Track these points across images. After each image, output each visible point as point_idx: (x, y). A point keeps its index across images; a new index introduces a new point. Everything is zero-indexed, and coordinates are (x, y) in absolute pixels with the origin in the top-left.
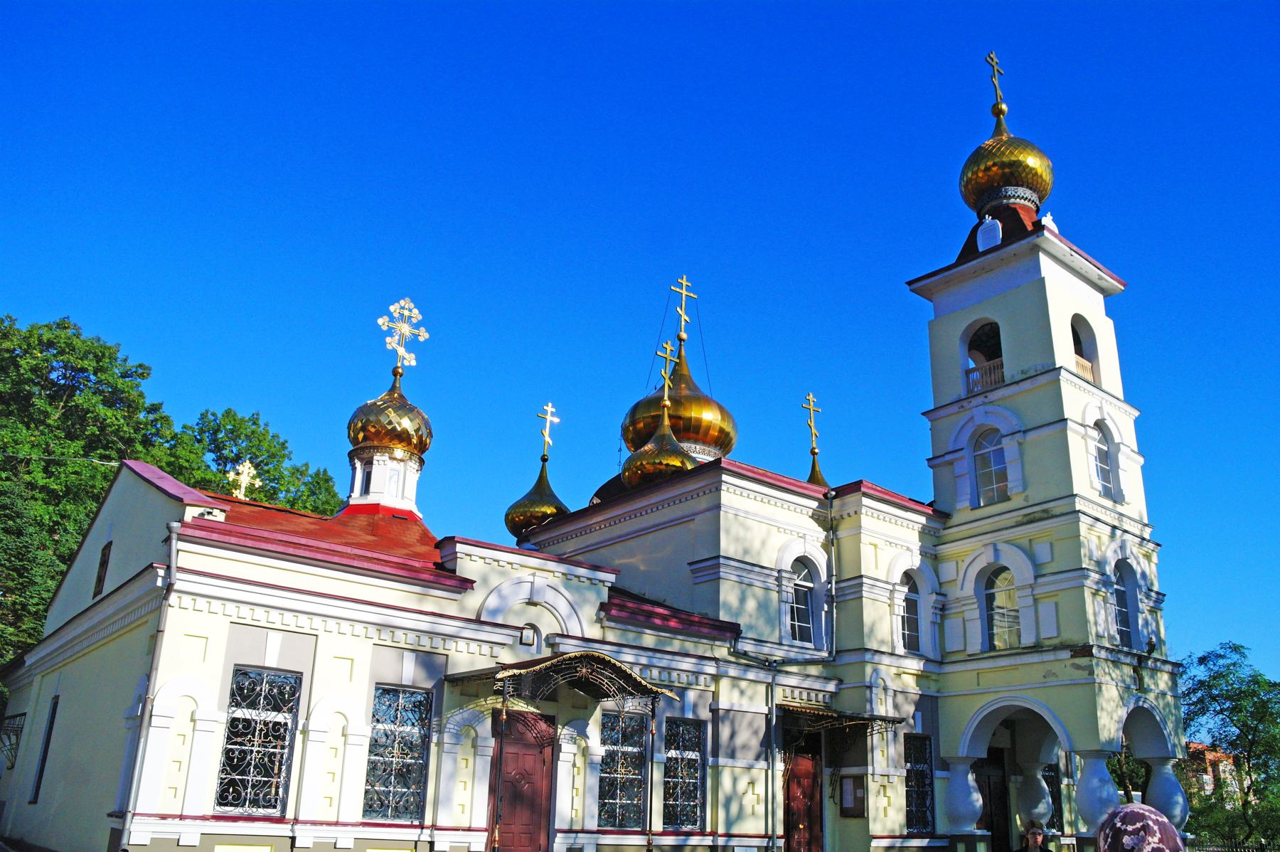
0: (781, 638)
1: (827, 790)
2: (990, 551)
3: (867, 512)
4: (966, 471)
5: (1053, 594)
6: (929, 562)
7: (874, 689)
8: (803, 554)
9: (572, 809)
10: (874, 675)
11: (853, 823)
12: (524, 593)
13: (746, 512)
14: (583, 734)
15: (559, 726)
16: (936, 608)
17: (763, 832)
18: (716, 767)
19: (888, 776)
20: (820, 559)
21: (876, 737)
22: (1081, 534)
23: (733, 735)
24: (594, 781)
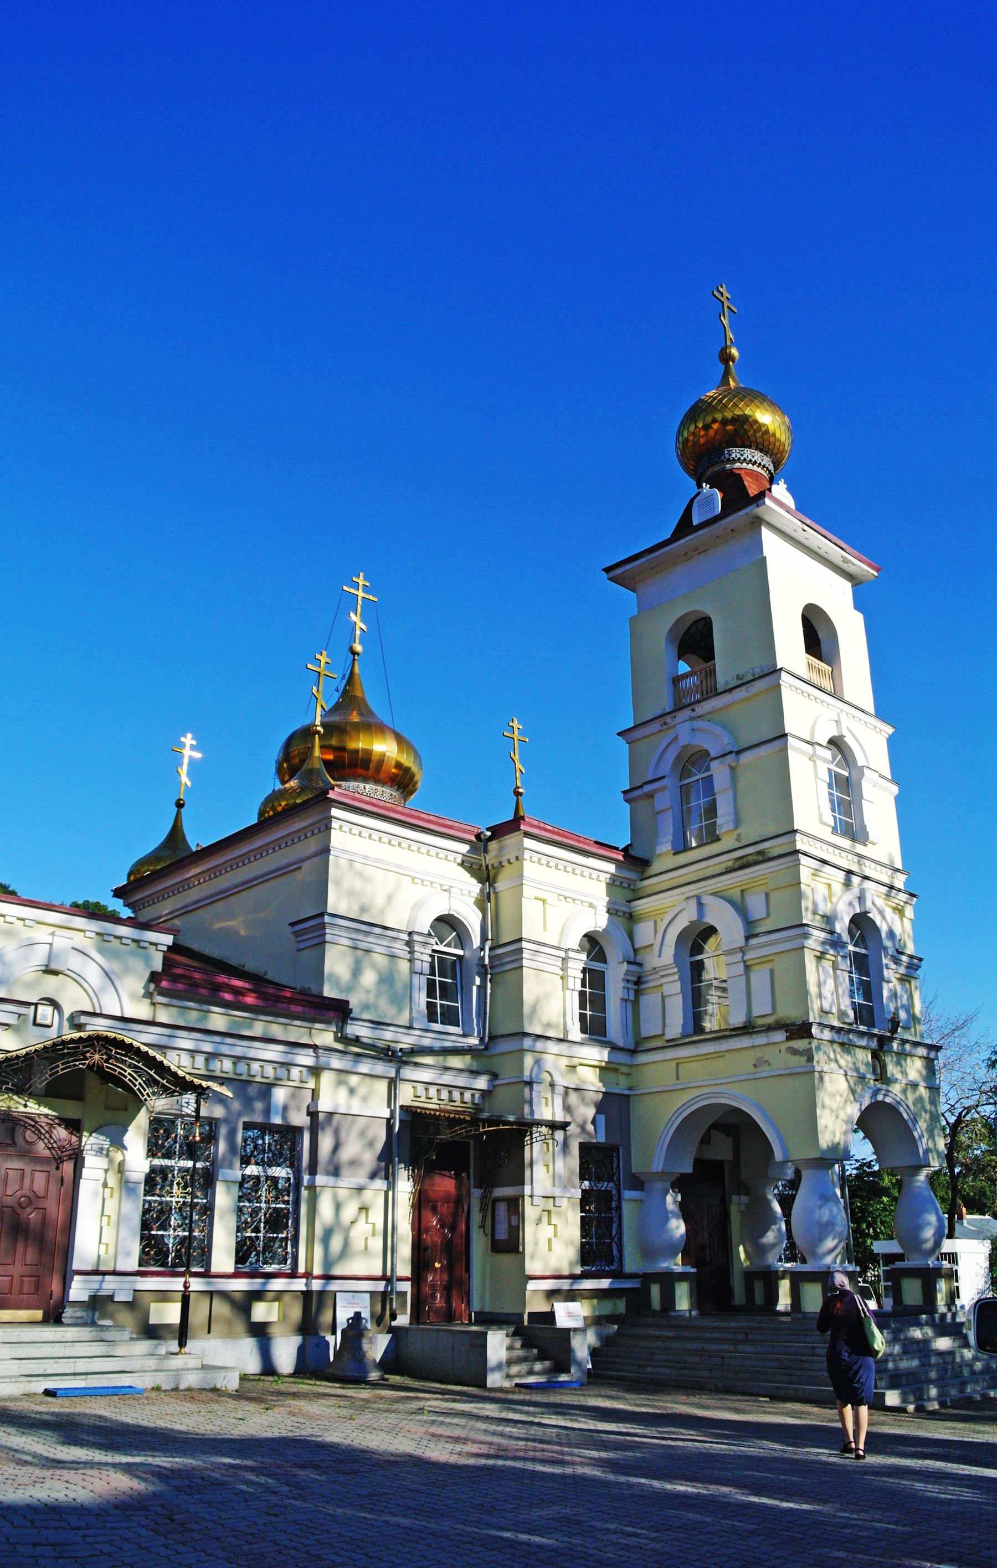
0: (411, 1020)
1: (476, 1217)
2: (693, 904)
3: (531, 857)
4: (668, 805)
5: (767, 960)
6: (620, 921)
7: (535, 1086)
8: (447, 913)
9: (100, 1243)
10: (536, 1067)
11: (505, 1260)
12: (39, 957)
13: (365, 857)
14: (119, 1144)
15: (85, 1133)
16: (628, 981)
17: (379, 1273)
18: (312, 1187)
19: (554, 1198)
20: (472, 919)
21: (536, 1146)
22: (802, 880)
23: (336, 1148)
24: (133, 1210)
